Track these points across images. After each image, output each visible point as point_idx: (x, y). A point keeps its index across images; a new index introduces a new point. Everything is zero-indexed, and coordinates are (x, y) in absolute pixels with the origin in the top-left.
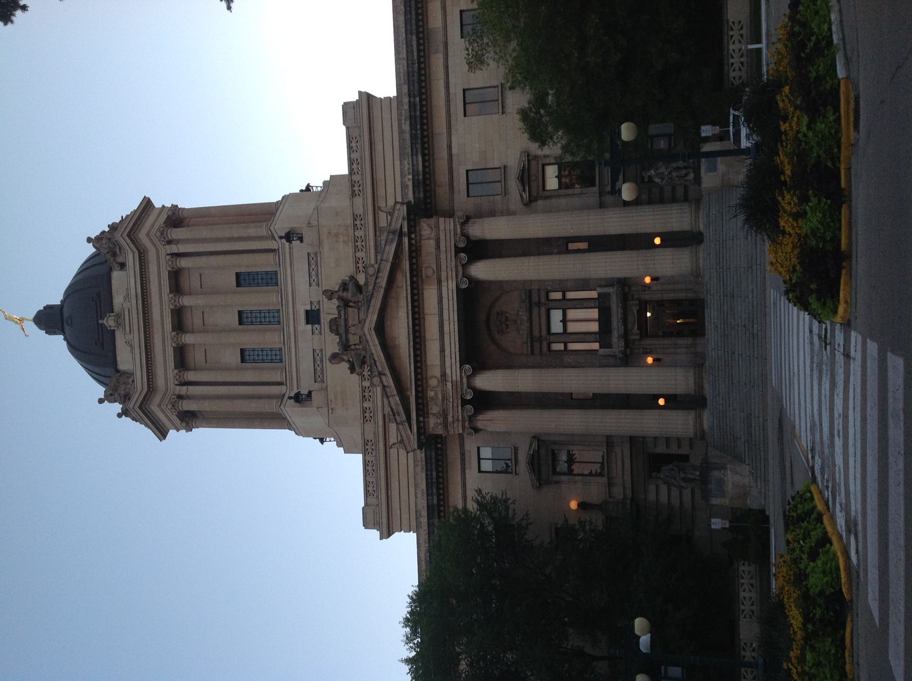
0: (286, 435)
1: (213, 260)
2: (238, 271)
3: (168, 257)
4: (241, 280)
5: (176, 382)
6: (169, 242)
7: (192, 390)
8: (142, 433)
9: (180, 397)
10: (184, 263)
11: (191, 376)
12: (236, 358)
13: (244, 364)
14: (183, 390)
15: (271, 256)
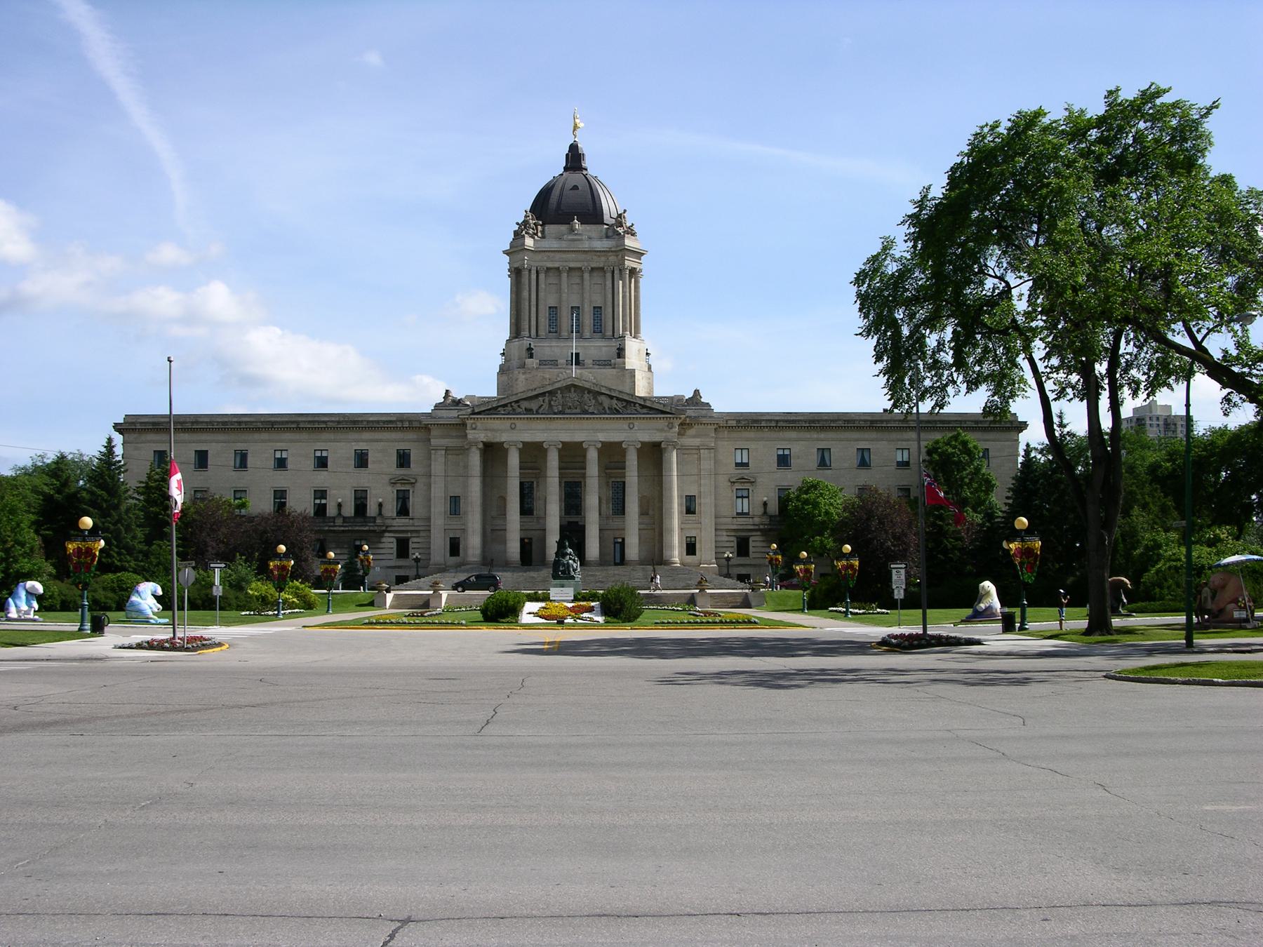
0: (507, 336)
1: (610, 296)
2: (603, 308)
3: (612, 268)
4: (598, 310)
5: (538, 268)
6: (620, 270)
7: (534, 276)
8: (506, 241)
9: (530, 271)
10: (609, 275)
11: (542, 276)
12: (552, 302)
13: (548, 308)
14: (534, 272)
15: (611, 333)
